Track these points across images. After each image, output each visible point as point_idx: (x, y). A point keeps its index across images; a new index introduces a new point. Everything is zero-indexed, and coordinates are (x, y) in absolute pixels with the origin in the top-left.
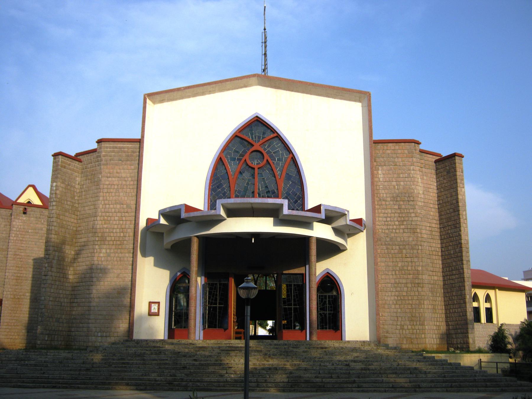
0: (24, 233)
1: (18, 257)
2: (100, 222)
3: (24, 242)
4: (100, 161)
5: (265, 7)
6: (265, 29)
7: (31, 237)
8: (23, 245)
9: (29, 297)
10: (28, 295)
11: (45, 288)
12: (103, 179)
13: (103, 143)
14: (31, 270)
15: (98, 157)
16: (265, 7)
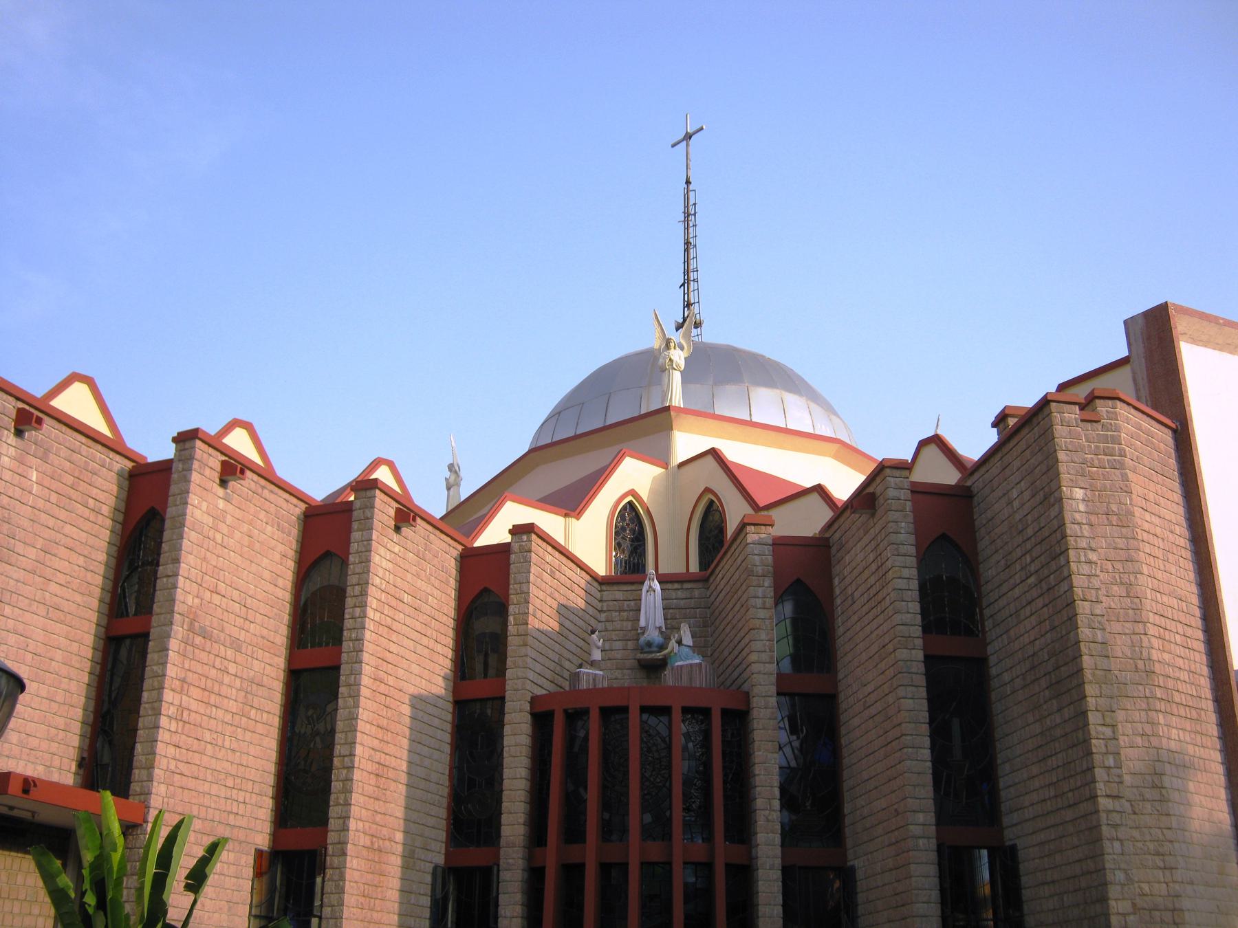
0: (394, 602)
1: (382, 688)
2: (1156, 643)
3: (394, 637)
4: (1120, 456)
6: (688, 182)
7: (409, 621)
8: (393, 648)
9: (399, 849)
10: (399, 836)
11: (1121, 841)
12: (1138, 512)
13: (1118, 403)
14: (405, 743)
15: (1105, 439)
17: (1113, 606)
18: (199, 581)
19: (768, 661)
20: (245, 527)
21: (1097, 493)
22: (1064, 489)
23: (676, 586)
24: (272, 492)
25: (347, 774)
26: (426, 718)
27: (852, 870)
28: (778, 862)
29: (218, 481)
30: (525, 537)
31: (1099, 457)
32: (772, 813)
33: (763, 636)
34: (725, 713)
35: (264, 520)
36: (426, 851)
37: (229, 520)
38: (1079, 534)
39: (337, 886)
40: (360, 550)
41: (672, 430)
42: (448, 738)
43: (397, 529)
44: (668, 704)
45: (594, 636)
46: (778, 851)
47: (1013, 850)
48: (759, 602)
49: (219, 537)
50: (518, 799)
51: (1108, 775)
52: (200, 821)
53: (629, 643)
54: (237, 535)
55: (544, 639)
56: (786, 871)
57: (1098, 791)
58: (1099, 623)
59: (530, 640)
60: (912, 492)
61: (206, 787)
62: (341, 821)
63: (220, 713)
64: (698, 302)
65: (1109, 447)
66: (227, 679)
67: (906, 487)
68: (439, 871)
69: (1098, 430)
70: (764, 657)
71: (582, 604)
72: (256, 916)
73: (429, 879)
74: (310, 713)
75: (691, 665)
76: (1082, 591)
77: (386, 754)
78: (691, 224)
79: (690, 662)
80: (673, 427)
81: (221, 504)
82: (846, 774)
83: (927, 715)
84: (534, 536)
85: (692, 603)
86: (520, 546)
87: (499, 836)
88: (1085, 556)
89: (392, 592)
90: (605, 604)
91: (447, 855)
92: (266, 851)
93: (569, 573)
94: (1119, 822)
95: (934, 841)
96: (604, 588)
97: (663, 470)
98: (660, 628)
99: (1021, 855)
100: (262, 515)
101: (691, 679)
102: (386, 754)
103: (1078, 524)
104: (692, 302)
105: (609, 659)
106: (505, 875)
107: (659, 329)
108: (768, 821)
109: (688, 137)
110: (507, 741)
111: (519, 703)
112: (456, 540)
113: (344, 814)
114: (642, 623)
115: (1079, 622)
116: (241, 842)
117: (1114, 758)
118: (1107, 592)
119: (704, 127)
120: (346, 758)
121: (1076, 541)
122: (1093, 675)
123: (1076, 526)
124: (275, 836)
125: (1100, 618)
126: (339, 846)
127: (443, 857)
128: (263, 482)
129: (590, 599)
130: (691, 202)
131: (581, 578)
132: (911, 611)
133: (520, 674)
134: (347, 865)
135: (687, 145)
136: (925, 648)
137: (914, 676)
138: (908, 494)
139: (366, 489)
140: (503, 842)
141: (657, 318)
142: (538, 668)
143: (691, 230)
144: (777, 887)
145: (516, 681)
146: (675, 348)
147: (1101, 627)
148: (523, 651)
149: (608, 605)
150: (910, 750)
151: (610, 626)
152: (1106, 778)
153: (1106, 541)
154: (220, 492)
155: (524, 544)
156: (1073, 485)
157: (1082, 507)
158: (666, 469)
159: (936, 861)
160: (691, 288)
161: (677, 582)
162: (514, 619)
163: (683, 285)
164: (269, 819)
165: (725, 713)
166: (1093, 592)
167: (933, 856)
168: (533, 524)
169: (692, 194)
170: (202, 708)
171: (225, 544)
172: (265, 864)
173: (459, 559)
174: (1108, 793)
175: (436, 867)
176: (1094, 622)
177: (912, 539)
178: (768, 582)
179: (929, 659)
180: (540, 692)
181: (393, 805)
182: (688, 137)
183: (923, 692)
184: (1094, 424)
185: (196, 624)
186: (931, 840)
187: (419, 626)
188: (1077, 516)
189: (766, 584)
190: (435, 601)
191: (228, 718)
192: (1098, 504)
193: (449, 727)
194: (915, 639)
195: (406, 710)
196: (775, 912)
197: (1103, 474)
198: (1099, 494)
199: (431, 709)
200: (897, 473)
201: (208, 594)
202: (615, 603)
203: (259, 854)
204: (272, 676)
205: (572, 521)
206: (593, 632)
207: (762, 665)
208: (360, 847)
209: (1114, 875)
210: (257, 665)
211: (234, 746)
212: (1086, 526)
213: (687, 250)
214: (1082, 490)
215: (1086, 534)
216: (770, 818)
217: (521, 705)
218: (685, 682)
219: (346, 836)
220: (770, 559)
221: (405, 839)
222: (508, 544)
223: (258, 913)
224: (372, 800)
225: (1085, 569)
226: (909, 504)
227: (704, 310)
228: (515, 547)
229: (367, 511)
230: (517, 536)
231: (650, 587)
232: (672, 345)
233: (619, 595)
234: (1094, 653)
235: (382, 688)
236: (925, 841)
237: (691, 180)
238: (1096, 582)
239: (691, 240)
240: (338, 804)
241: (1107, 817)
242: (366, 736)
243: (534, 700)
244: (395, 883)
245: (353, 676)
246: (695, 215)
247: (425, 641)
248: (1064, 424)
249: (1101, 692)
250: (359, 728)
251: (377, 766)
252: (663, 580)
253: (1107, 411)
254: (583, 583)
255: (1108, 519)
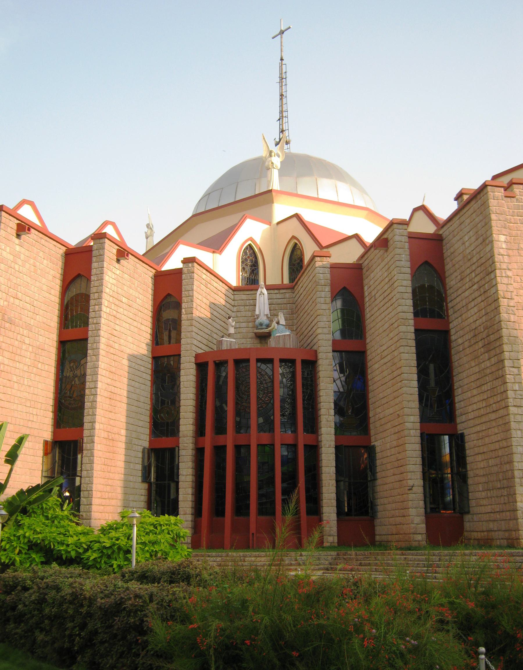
0: (117, 302)
1: (112, 350)
5: (290, 28)
6: (282, 59)
7: (126, 313)
8: (117, 328)
9: (123, 439)
10: (123, 432)
14: (125, 380)
16: (290, 28)
17: (520, 301)
18: (7, 292)
19: (327, 333)
20: (32, 261)
21: (513, 238)
22: (494, 235)
23: (276, 291)
24: (46, 241)
25: (93, 398)
26: (137, 367)
27: (374, 447)
28: (333, 444)
29: (15, 235)
30: (190, 265)
31: (515, 217)
32: (330, 417)
33: (325, 319)
34: (304, 362)
35: (42, 257)
36: (138, 440)
37: (22, 256)
38: (502, 261)
39: (90, 460)
40: (97, 273)
41: (273, 203)
42: (149, 378)
43: (118, 261)
44: (272, 357)
45: (230, 320)
46: (333, 437)
47: (462, 435)
48: (322, 300)
49: (17, 267)
50: (189, 411)
51: (515, 394)
52: (12, 425)
53: (250, 324)
54: (27, 265)
55: (202, 322)
56: (337, 448)
57: (510, 403)
58: (512, 310)
59: (194, 323)
60: (409, 237)
61: (15, 407)
62: (91, 424)
63: (21, 366)
64: (288, 130)
65: (520, 212)
66: (24, 347)
67: (406, 235)
68: (146, 451)
69: (514, 202)
70: (326, 331)
71: (223, 302)
72: (45, 477)
73: (140, 455)
74: (72, 364)
75: (284, 335)
76: (503, 293)
77: (115, 387)
78: (284, 84)
79: (284, 334)
80: (274, 201)
81: (18, 248)
82: (371, 395)
83: (415, 362)
84: (195, 264)
85: (285, 301)
86: (188, 269)
87: (178, 431)
88: (505, 273)
89: (116, 297)
90: (236, 302)
91: (150, 441)
92: (50, 441)
93: (215, 285)
94: (520, 420)
95: (419, 431)
96: (235, 293)
97: (269, 226)
98: (267, 315)
99: (467, 438)
100: (41, 254)
101: (284, 344)
102: (115, 387)
103: (502, 255)
104: (285, 129)
105: (239, 333)
106: (182, 452)
107: (265, 145)
108: (328, 421)
109: (282, 32)
110: (182, 379)
111: (188, 358)
112: (151, 267)
113: (92, 420)
114: (257, 312)
115: (501, 310)
116: (35, 437)
117: (519, 385)
118: (517, 293)
119: (291, 27)
120: (92, 390)
121: (500, 265)
122: (508, 340)
123: (500, 256)
124: (55, 433)
125: (513, 308)
126: (90, 438)
127: (148, 443)
128: (41, 235)
129: (228, 299)
130: (284, 71)
131: (223, 288)
132: (407, 304)
133: (189, 342)
134: (95, 448)
135: (281, 37)
136: (415, 325)
137: (409, 341)
138: (406, 239)
139: (100, 239)
140: (181, 434)
141: (264, 138)
142: (199, 338)
143: (284, 87)
144: (333, 457)
145: (187, 346)
146: (274, 156)
147: (513, 313)
148: (190, 328)
149: (238, 303)
150: (406, 381)
151: (239, 314)
152: (514, 397)
153: (517, 265)
154: (17, 241)
155: (190, 268)
156: (500, 233)
157: (504, 246)
158: (270, 225)
159: (420, 442)
160: (284, 122)
161: (276, 289)
162: (185, 311)
163: (279, 120)
164: (51, 424)
165: (304, 362)
166: (509, 293)
167: (418, 439)
168: (195, 257)
169: (284, 66)
170: (11, 363)
171: (21, 271)
172: (49, 448)
173: (153, 278)
174: (515, 405)
175: (144, 448)
176: (509, 310)
177: (408, 264)
178: (328, 289)
179: (417, 331)
180: (200, 351)
181: (119, 415)
182: (282, 32)
183: (414, 350)
184: (512, 198)
185: (6, 316)
186: (417, 431)
187: (131, 315)
188: (502, 251)
189: (326, 290)
190: (140, 301)
191: (26, 368)
192: (513, 244)
193: (149, 372)
194: (410, 320)
195: (126, 362)
196: (331, 470)
197: (516, 227)
198: (514, 239)
199: (139, 362)
200: (400, 227)
201: (12, 299)
202: (242, 301)
203: (46, 443)
204: (50, 344)
205: (217, 255)
206: (229, 318)
207: (324, 335)
208: (101, 438)
209: (517, 449)
210: (41, 339)
211: (30, 384)
212: (506, 257)
213: (281, 99)
214: (504, 236)
215: (506, 261)
216: (329, 419)
217: (189, 359)
218: (281, 345)
219: (94, 432)
220: (328, 276)
221: (127, 433)
222: (181, 269)
223: (46, 475)
224: (108, 412)
225: (505, 280)
226: (407, 244)
227: (292, 134)
228: (185, 270)
229: (100, 251)
230: (186, 264)
231: (261, 292)
232: (273, 154)
233: (244, 297)
234: (509, 328)
235: (112, 350)
236: (414, 431)
237: (283, 58)
238: (511, 288)
239: (284, 94)
240: (89, 415)
241: (514, 417)
242: (103, 377)
243: (197, 356)
244: (122, 458)
245: (95, 344)
246: (286, 78)
247: (135, 324)
248: (495, 198)
249: (512, 349)
250: (99, 373)
251: (110, 393)
252: (269, 288)
253: (520, 191)
254: (223, 290)
255: (519, 253)
